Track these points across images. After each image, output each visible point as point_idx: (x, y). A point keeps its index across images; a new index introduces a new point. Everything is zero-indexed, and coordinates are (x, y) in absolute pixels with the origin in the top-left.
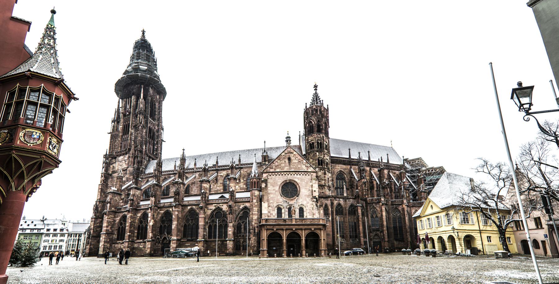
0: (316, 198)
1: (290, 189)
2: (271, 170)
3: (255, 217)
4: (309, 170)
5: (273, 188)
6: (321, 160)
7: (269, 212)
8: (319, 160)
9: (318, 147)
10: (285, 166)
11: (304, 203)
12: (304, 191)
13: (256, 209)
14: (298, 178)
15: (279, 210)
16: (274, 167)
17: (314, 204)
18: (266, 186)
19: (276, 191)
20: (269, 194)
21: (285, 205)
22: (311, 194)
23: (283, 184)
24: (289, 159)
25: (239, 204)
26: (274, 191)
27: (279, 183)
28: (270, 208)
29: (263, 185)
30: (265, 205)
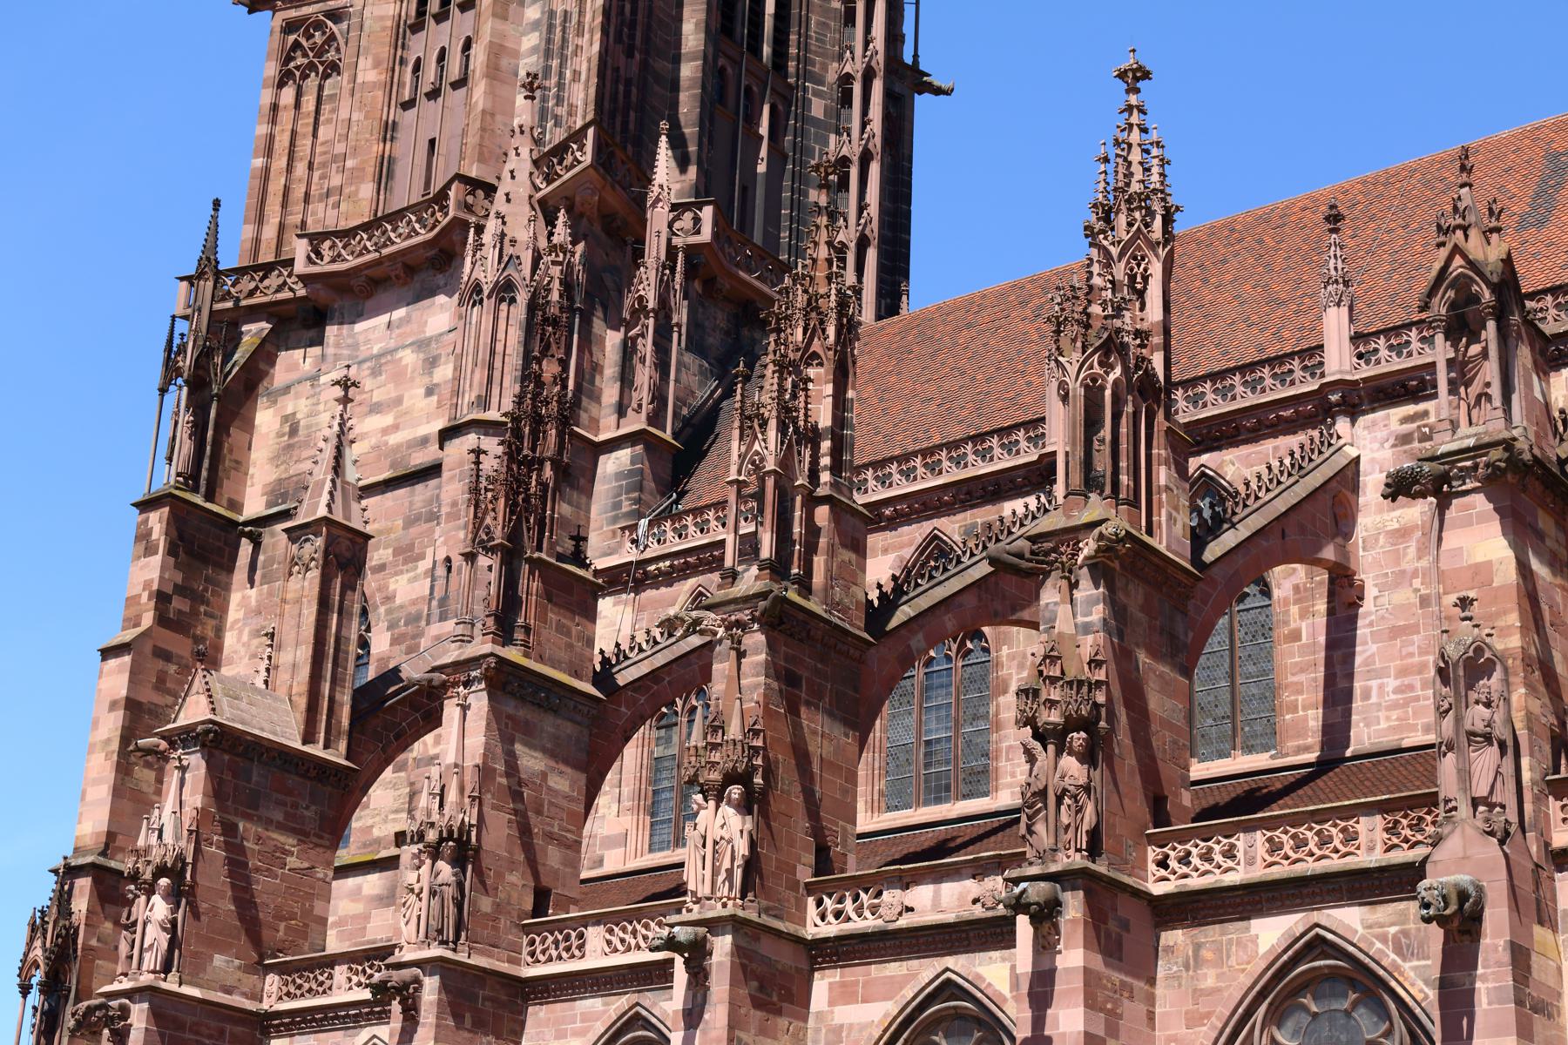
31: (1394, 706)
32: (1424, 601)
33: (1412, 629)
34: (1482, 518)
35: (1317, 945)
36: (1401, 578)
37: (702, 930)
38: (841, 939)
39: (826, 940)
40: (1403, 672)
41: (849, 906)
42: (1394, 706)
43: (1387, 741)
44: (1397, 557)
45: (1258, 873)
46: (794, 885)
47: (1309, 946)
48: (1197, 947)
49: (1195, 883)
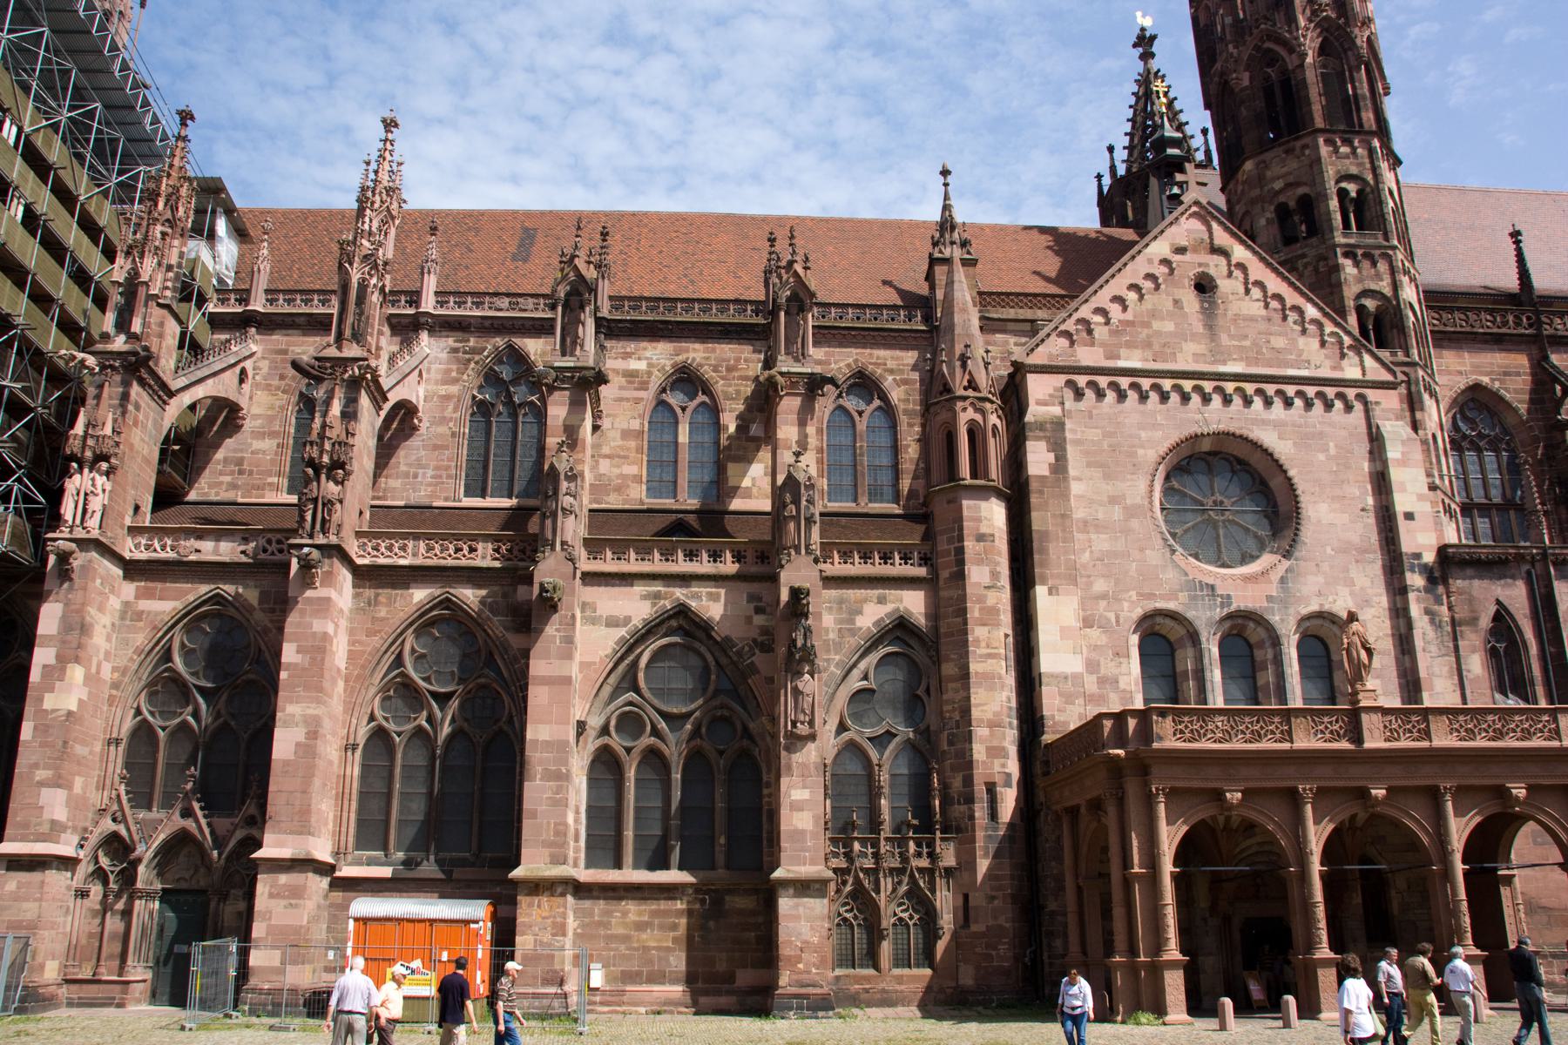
1: (1227, 497)
2: (1088, 356)
4: (1353, 372)
5: (1107, 488)
6: (1378, 318)
7: (1092, 666)
8: (1360, 310)
9: (1346, 225)
10: (1182, 335)
14: (1278, 425)
15: (1162, 640)
16: (1100, 332)
18: (1060, 466)
19: (1130, 512)
21: (1206, 618)
24: (1204, 286)
26: (1117, 513)
27: (1150, 455)
29: (1038, 459)
30: (1054, 610)
31: (430, 485)
32: (453, 435)
33: (446, 447)
34: (563, 404)
35: (447, 603)
36: (444, 420)
37: (74, 545)
38: (149, 562)
39: (138, 561)
40: (437, 468)
41: (157, 545)
42: (430, 485)
43: (425, 501)
44: (443, 409)
45: (419, 561)
46: (122, 526)
47: (441, 602)
48: (377, 595)
49: (382, 561)
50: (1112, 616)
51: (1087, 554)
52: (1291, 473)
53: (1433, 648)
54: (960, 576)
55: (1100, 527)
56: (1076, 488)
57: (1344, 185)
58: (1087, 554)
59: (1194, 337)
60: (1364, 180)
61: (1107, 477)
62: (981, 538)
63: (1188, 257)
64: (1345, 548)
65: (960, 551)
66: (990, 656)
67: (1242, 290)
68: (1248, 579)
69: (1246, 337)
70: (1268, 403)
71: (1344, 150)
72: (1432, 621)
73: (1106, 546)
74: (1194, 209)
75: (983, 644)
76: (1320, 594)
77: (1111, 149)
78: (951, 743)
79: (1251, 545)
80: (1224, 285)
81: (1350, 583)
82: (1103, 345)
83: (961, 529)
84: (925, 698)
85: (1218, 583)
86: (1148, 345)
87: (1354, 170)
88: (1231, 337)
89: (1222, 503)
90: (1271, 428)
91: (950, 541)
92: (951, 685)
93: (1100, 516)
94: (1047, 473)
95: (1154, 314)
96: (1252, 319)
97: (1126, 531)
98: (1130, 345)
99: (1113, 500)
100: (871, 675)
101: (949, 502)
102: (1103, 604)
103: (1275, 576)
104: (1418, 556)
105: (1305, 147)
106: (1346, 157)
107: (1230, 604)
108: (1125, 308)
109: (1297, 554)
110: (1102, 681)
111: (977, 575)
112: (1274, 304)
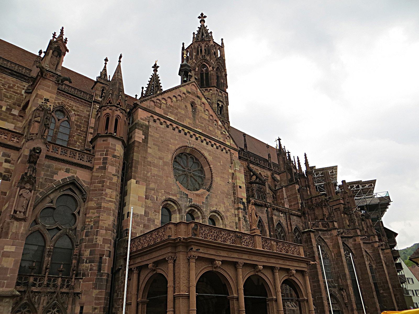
0: (243, 203)
3: (108, 220)
4: (228, 144)
5: (159, 154)
7: (146, 213)
11: (221, 209)
12: (220, 183)
13: (112, 195)
14: (209, 151)
17: (241, 216)
18: (146, 140)
19: (165, 164)
20: (150, 164)
21: (184, 204)
22: (231, 192)
23: (178, 152)
25: (55, 164)
27: (173, 148)
28: (149, 201)
29: (138, 136)
50: (155, 197)
51: (150, 173)
52: (211, 166)
53: (245, 228)
54: (104, 168)
55: (155, 166)
56: (149, 151)
57: (219, 102)
58: (150, 173)
59: (189, 118)
60: (223, 103)
61: (159, 150)
62: (114, 156)
63: (190, 95)
64: (223, 193)
65: (105, 159)
66: (110, 201)
67: (203, 110)
68: (197, 195)
69: (203, 123)
70: (207, 144)
71: (220, 94)
72: (245, 219)
73: (156, 173)
74: (194, 83)
75: (108, 196)
76: (216, 205)
77: (143, 88)
78: (87, 236)
79: (197, 186)
80: (199, 107)
81: (224, 203)
82: (163, 109)
83: (107, 151)
84: (77, 215)
85: (189, 194)
86: (176, 115)
87: (221, 100)
88: (199, 122)
89: (190, 170)
90: (208, 151)
91: (102, 155)
92: (91, 211)
93: (155, 162)
94: (141, 142)
95: (179, 107)
96: (205, 119)
97: (163, 170)
98: (171, 112)
99: (160, 158)
100: (55, 201)
101: (103, 141)
102: (153, 192)
103: (205, 197)
104: (242, 199)
105: (211, 90)
106: (220, 96)
107: (192, 202)
108: (172, 102)
109: (211, 191)
110: (149, 220)
111: (112, 169)
112: (211, 118)
